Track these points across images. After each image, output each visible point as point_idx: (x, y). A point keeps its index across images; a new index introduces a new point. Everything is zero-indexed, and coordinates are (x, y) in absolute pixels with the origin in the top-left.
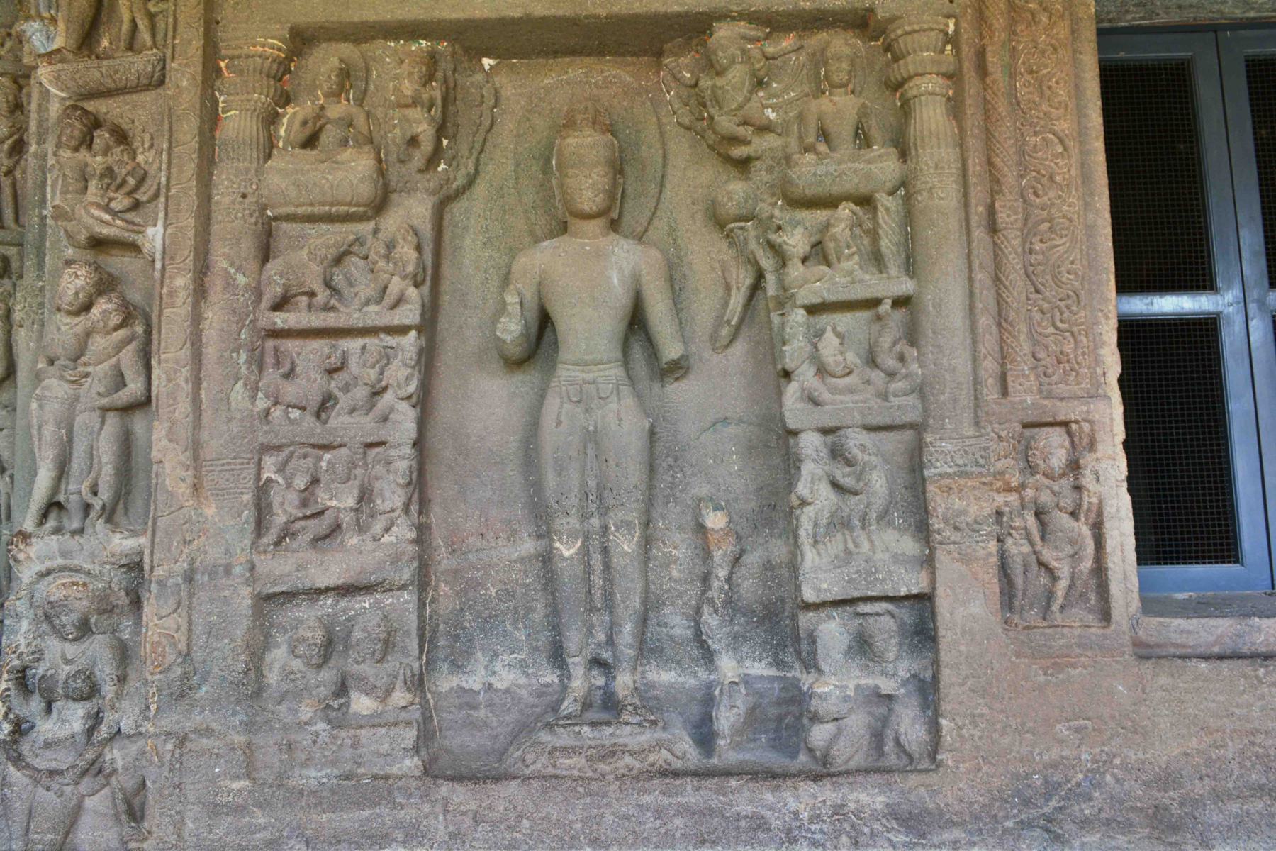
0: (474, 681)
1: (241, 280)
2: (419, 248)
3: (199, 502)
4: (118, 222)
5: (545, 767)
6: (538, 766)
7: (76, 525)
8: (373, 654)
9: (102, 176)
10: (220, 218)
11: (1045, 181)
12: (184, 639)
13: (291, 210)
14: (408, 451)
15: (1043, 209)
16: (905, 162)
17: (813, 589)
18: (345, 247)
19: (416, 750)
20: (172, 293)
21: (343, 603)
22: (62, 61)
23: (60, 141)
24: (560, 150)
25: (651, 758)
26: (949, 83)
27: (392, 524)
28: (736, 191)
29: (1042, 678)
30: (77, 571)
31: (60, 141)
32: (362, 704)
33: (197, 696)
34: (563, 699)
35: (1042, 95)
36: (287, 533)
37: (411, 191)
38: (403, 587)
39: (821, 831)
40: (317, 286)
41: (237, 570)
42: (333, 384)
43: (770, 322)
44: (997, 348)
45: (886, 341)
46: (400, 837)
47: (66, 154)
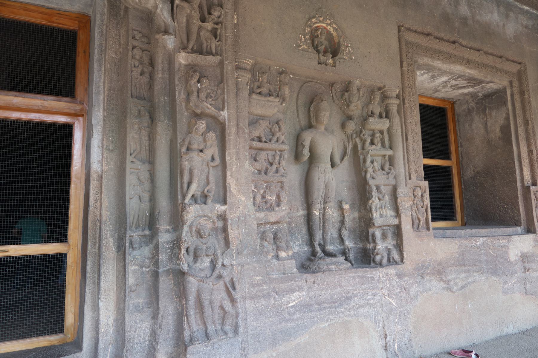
46: (297, 289)
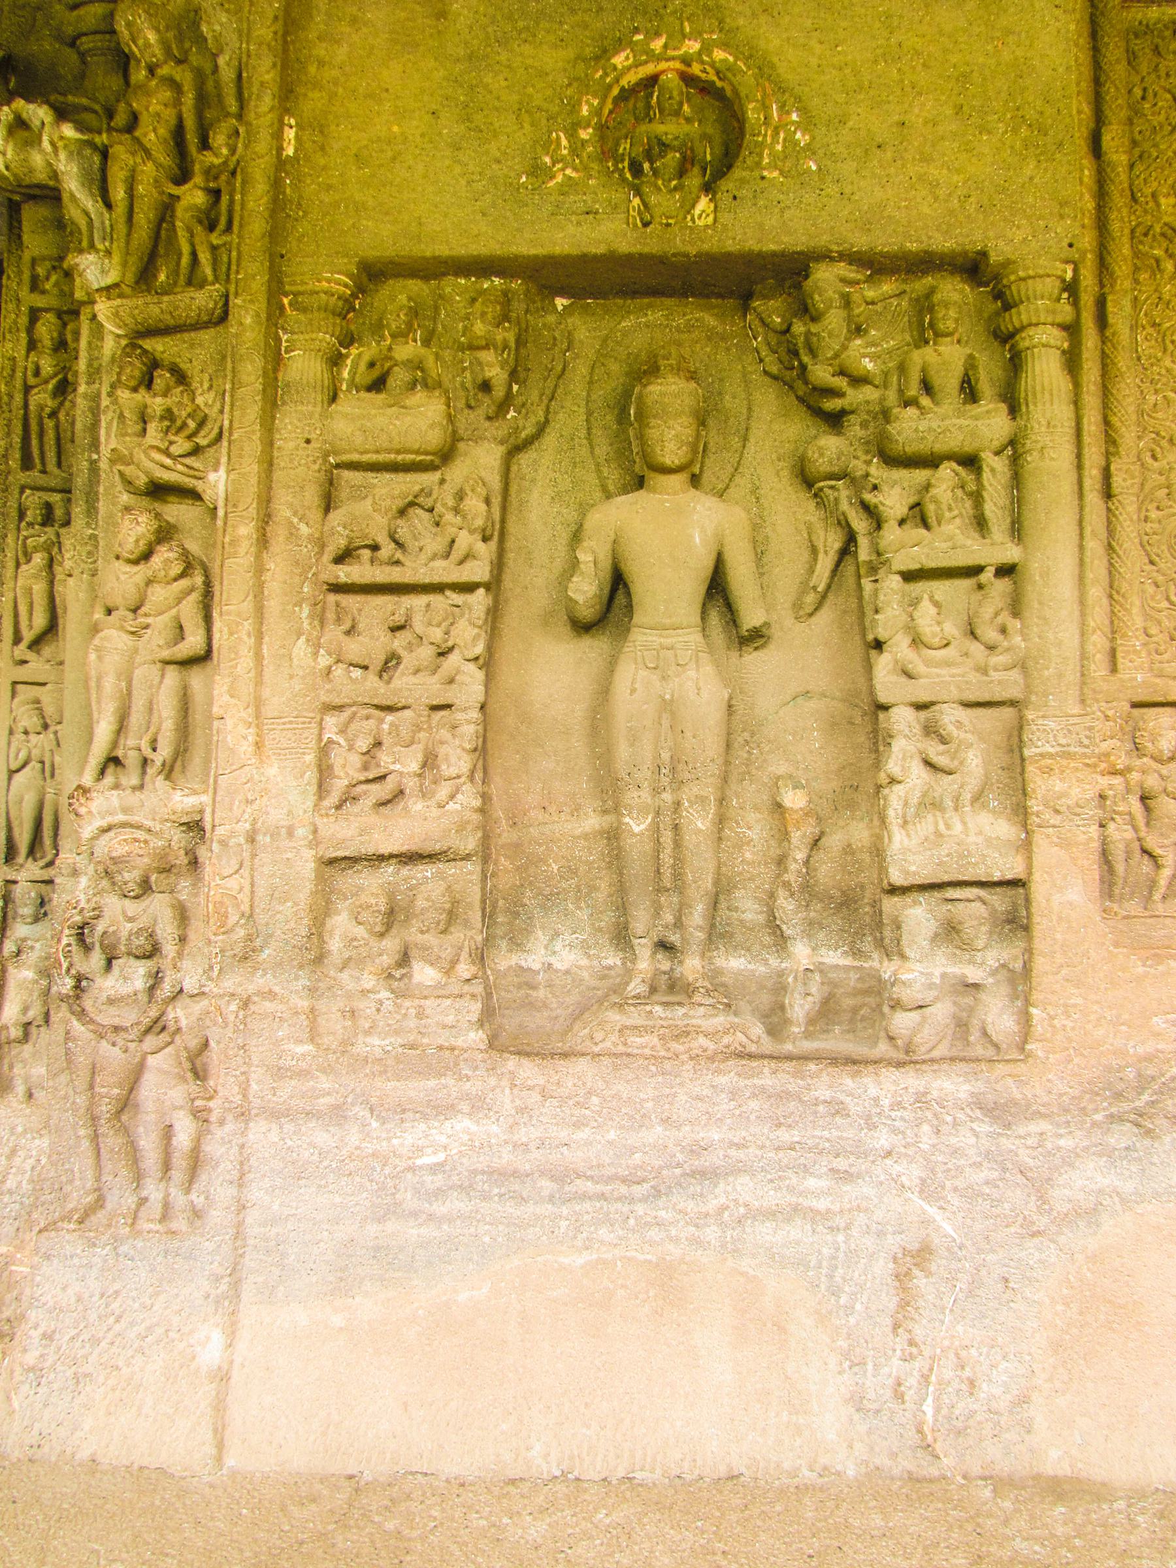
0: (534, 960)
1: (304, 530)
2: (487, 501)
3: (262, 762)
4: (180, 467)
5: (615, 1044)
6: (608, 1044)
7: (135, 781)
8: (438, 923)
9: (162, 418)
10: (282, 464)
11: (1164, 443)
12: (247, 900)
13: (355, 457)
14: (475, 714)
15: (1161, 474)
16: (1014, 419)
17: (901, 871)
18: (410, 498)
19: (481, 1023)
20: (233, 543)
21: (405, 871)
22: (121, 296)
23: (119, 380)
24: (640, 397)
25: (726, 1040)
26: (1064, 334)
27: (457, 790)
28: (829, 448)
29: (1140, 970)
30: (139, 827)
31: (119, 380)
32: (424, 974)
33: (260, 959)
34: (627, 984)
35: (1165, 350)
36: (348, 798)
37: (477, 439)
38: (467, 857)
39: (902, 1119)
40: (382, 539)
41: (300, 832)
42: (396, 643)
43: (860, 587)
44: (1107, 622)
45: (987, 611)
46: (465, 1107)
47: (124, 395)
